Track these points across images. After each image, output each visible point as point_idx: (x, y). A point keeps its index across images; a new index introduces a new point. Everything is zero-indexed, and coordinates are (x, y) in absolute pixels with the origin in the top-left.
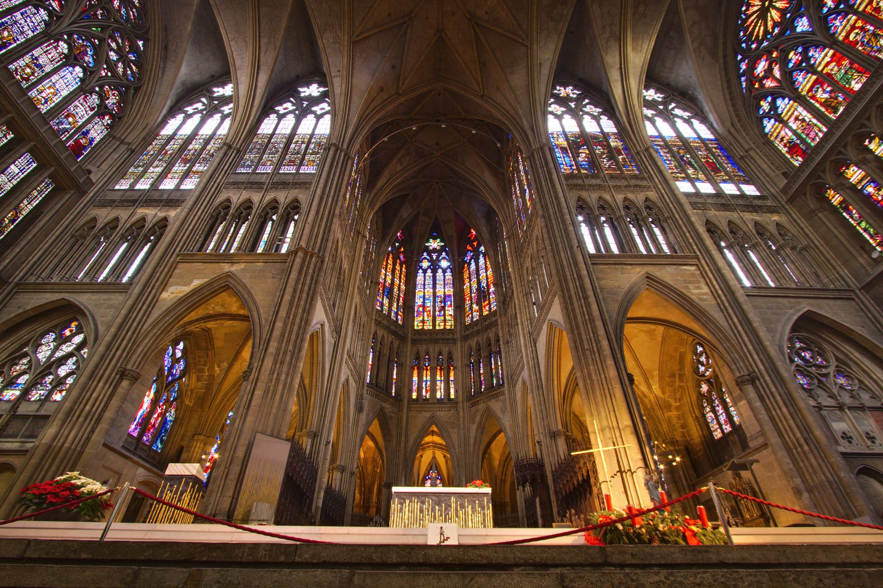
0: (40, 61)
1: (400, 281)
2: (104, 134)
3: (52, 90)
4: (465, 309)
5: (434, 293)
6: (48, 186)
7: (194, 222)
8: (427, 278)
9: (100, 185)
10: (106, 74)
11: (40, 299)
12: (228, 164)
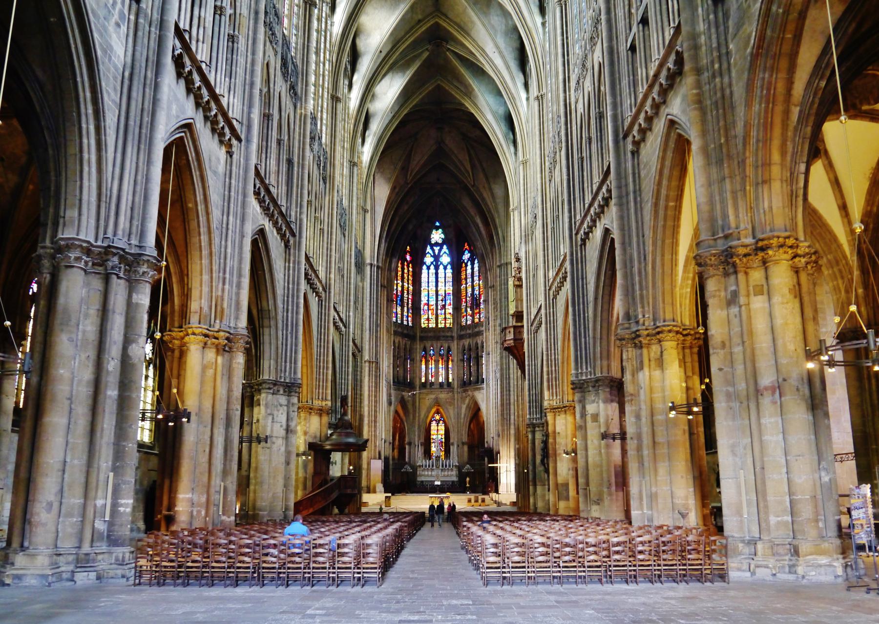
1: (408, 284)
4: (461, 309)
5: (437, 291)
8: (430, 275)
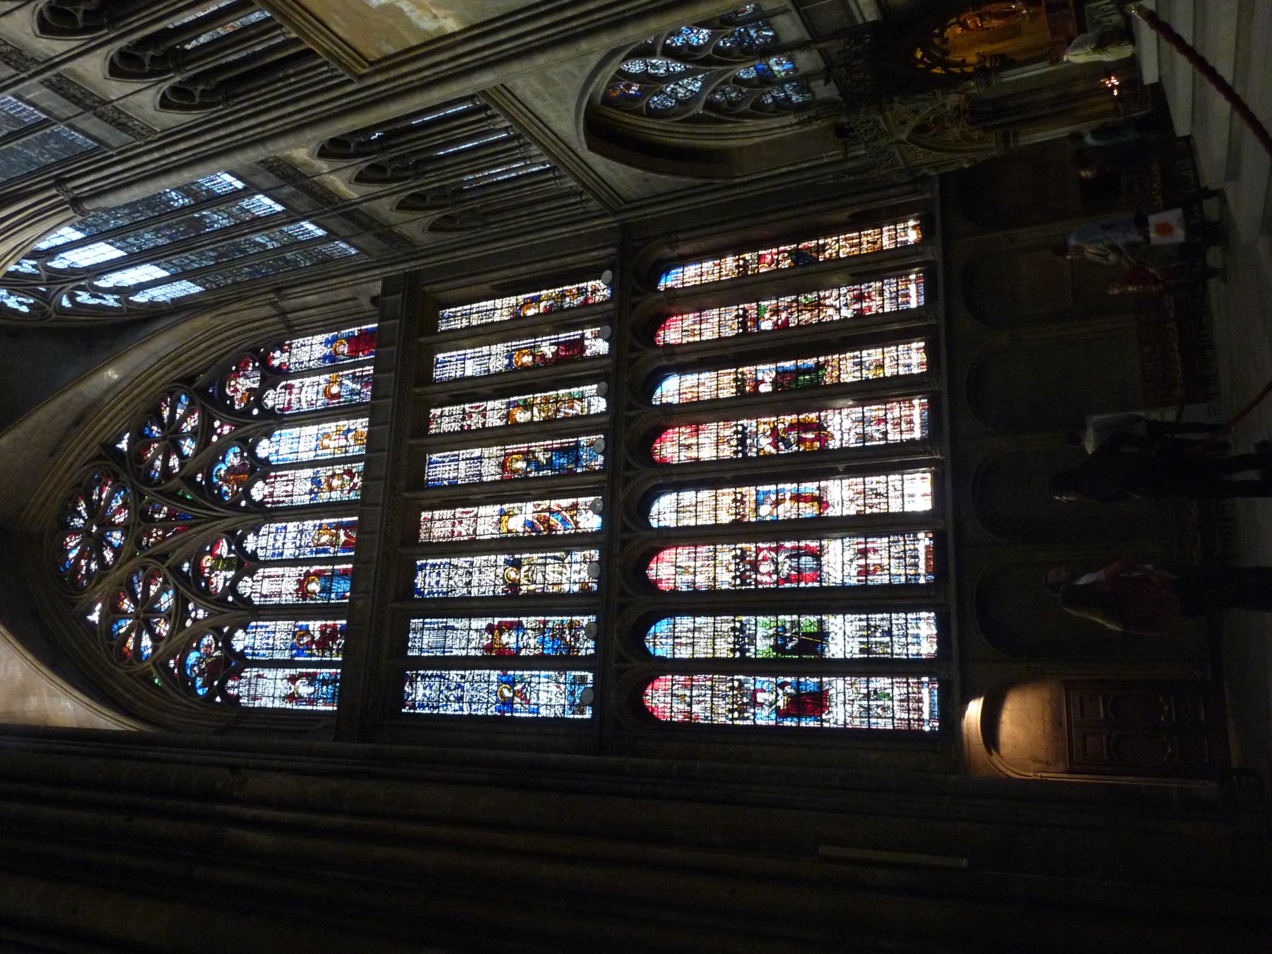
0: (309, 486)
2: (301, 340)
3: (326, 442)
6: (449, 317)
7: (275, 114)
9: (377, 272)
10: (221, 426)
11: (613, 171)
12: (106, 173)
